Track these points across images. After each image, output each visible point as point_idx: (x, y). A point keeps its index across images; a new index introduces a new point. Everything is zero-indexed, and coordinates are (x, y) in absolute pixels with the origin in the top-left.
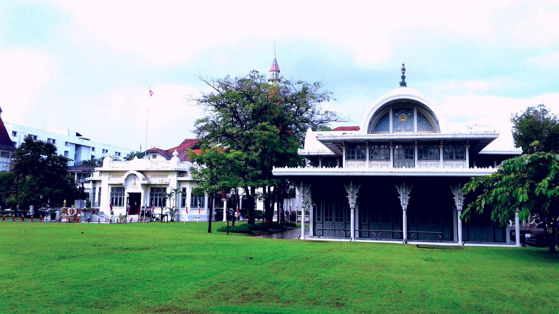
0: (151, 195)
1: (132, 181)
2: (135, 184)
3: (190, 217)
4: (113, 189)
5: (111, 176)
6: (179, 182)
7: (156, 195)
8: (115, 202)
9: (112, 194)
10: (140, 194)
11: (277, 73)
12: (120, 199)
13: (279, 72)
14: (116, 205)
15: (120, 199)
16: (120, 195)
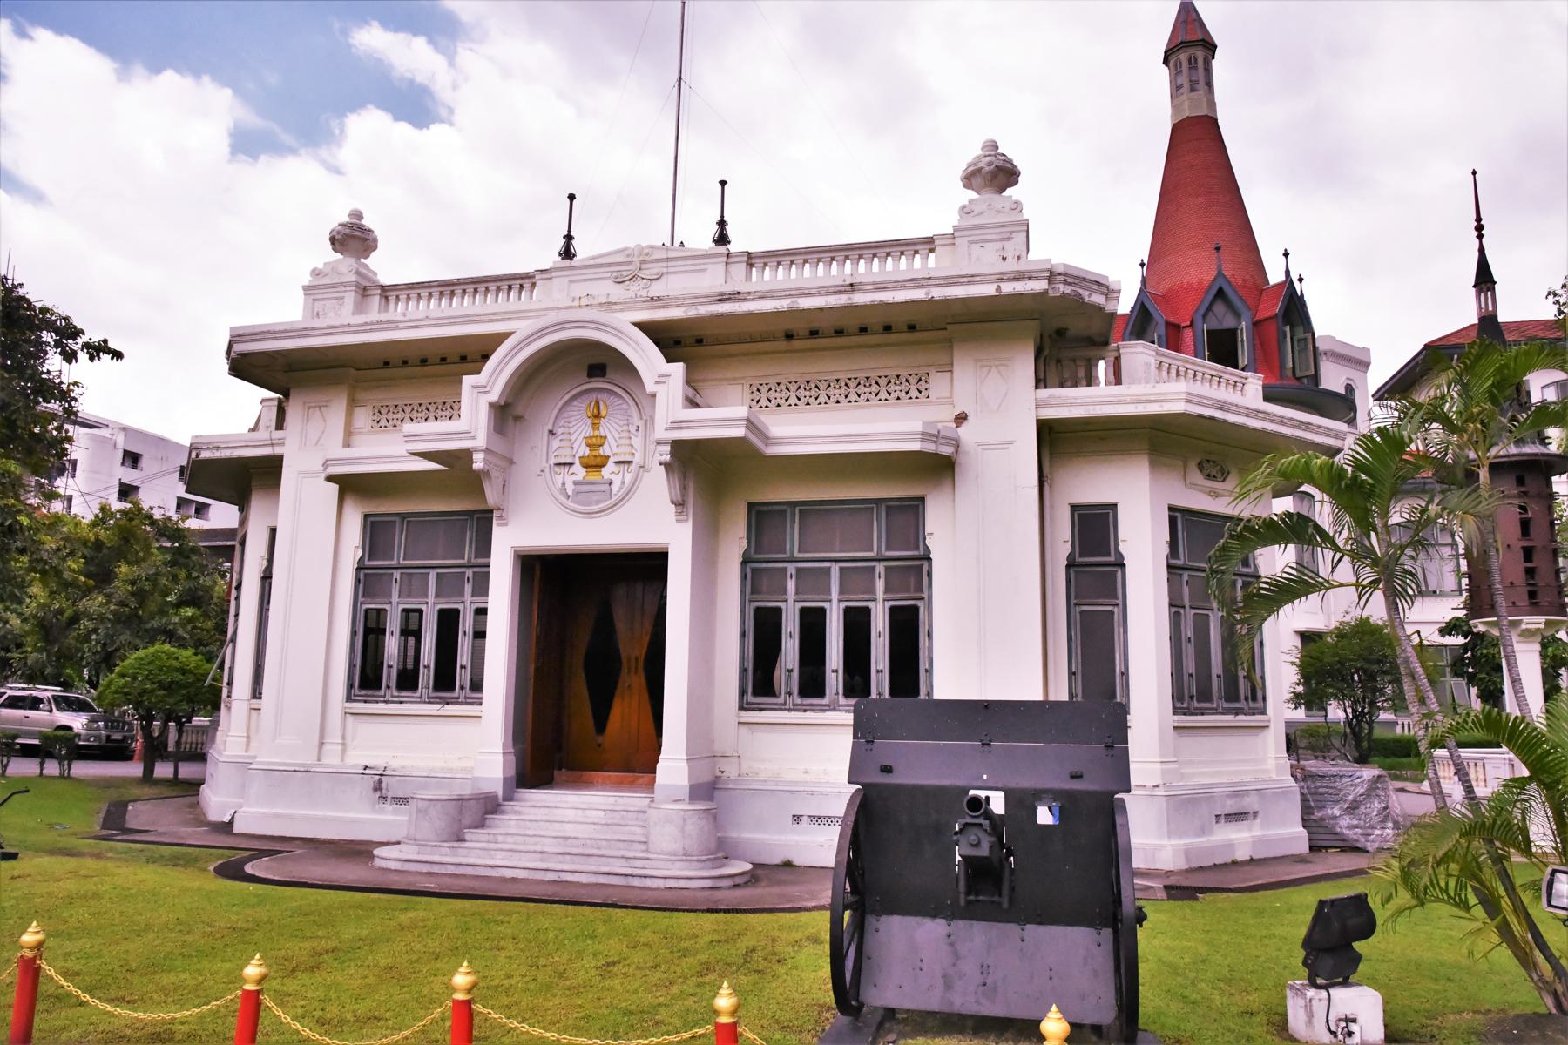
0: (755, 575)
1: (565, 431)
2: (594, 464)
3: (1186, 806)
4: (376, 533)
5: (363, 417)
6: (1056, 441)
7: (813, 579)
8: (398, 660)
9: (368, 580)
10: (648, 567)
11: (1200, 54)
12: (448, 621)
13: (1210, 47)
14: (408, 680)
15: (448, 621)
16: (449, 584)
